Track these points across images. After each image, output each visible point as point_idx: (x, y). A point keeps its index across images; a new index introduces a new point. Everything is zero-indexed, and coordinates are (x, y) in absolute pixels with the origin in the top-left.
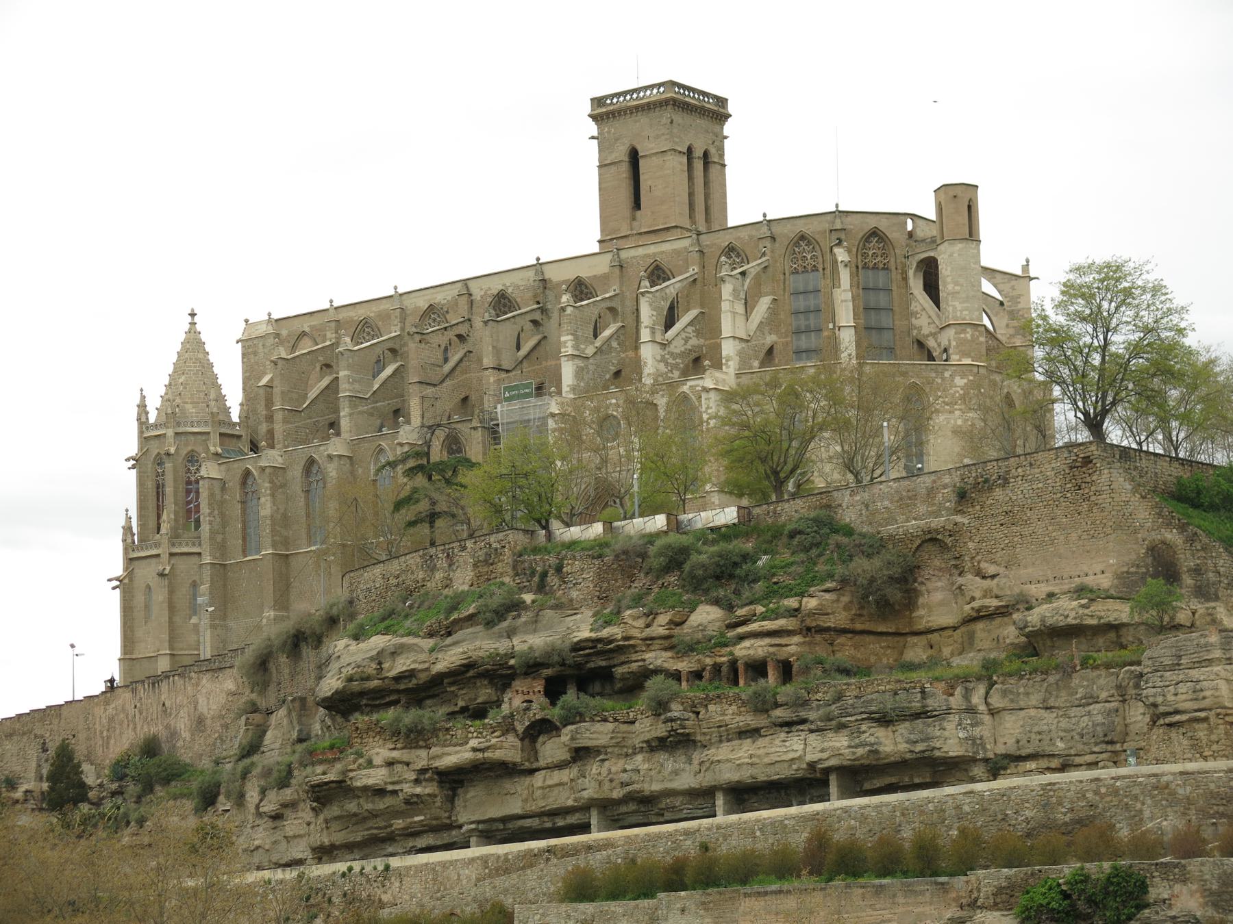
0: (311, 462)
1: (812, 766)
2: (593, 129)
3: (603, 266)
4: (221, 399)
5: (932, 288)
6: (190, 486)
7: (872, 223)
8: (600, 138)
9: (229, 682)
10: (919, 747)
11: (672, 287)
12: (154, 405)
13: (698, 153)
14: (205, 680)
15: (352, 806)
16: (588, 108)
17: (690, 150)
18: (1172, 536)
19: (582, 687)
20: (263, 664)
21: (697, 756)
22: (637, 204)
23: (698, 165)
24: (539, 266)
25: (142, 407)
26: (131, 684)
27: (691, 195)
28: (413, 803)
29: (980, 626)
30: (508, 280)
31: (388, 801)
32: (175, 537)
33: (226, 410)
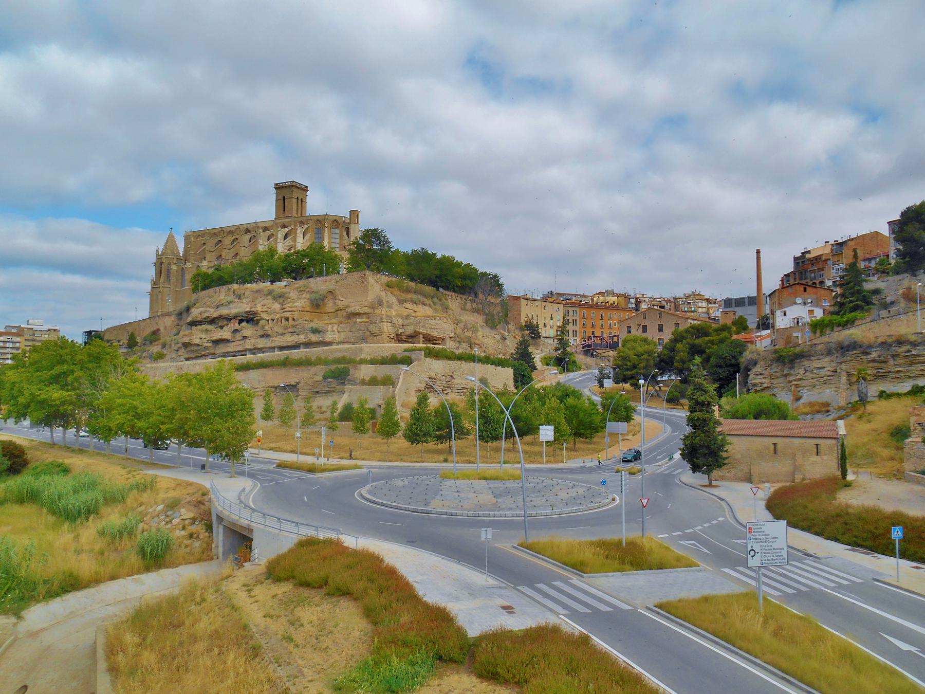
0: (198, 266)
1: (296, 342)
2: (275, 191)
3: (271, 224)
4: (178, 250)
5: (348, 234)
6: (169, 270)
7: (335, 218)
8: (276, 193)
9: (173, 318)
10: (321, 339)
11: (286, 230)
12: (160, 250)
14: (167, 317)
15: (192, 348)
18: (383, 293)
19: (248, 322)
20: (180, 314)
21: (271, 339)
22: (284, 210)
23: (300, 202)
25: (157, 251)
26: (150, 318)
27: (297, 209)
28: (206, 348)
29: (339, 312)
30: (249, 225)
31: (200, 347)
32: (164, 283)
33: (179, 253)
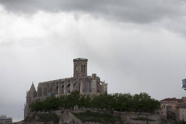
2: (73, 62)
3: (65, 80)
13: (83, 65)
16: (73, 60)
17: (82, 65)
23: (83, 67)
24: (60, 80)
25: (27, 92)
